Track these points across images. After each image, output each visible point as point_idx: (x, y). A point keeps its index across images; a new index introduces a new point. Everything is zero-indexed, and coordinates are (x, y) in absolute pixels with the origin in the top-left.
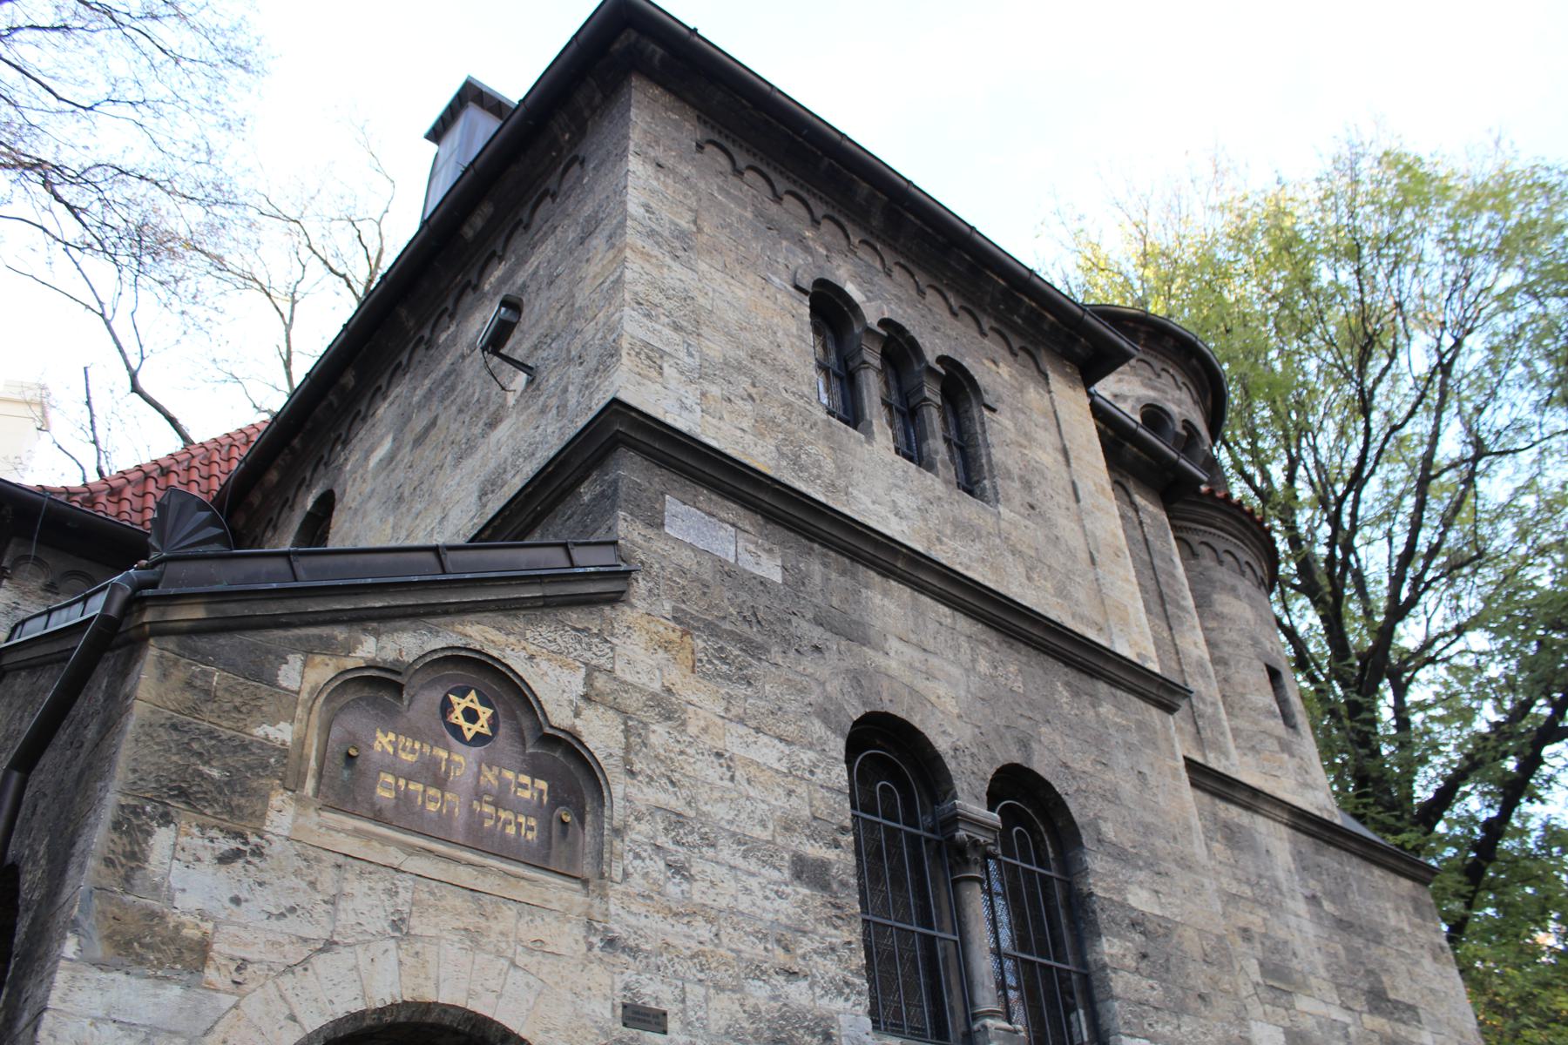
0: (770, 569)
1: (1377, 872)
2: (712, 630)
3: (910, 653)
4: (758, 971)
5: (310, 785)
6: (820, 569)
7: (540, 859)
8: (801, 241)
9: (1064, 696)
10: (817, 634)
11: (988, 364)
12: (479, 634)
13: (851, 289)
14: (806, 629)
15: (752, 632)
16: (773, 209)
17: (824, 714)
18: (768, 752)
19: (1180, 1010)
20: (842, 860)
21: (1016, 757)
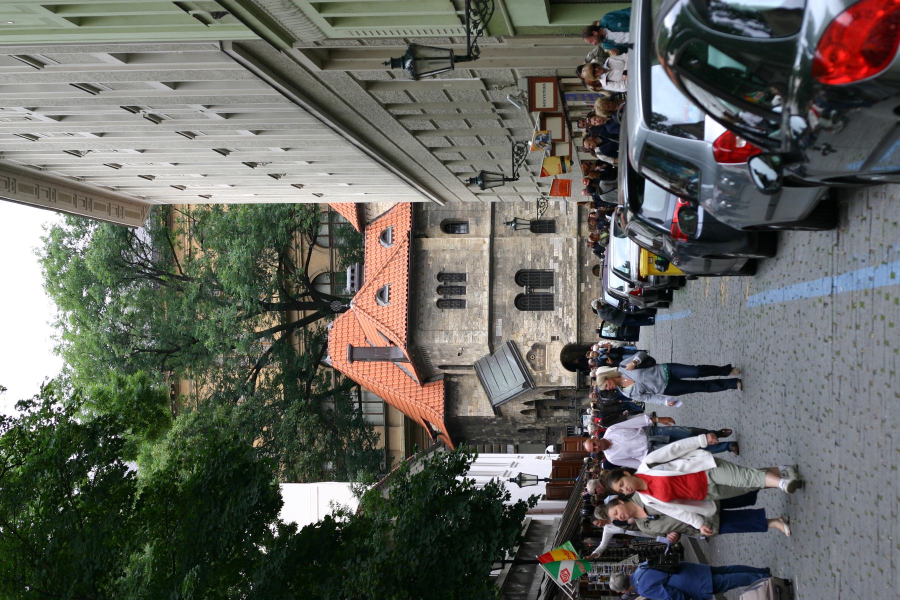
0: (500, 320)
2: (512, 330)
3: (504, 297)
4: (551, 325)
6: (497, 312)
7: (545, 349)
8: (430, 310)
9: (499, 266)
10: (507, 314)
12: (524, 357)
13: (435, 300)
14: (507, 315)
16: (426, 315)
17: (518, 314)
18: (526, 322)
19: (544, 254)
20: (536, 313)
21: (513, 280)
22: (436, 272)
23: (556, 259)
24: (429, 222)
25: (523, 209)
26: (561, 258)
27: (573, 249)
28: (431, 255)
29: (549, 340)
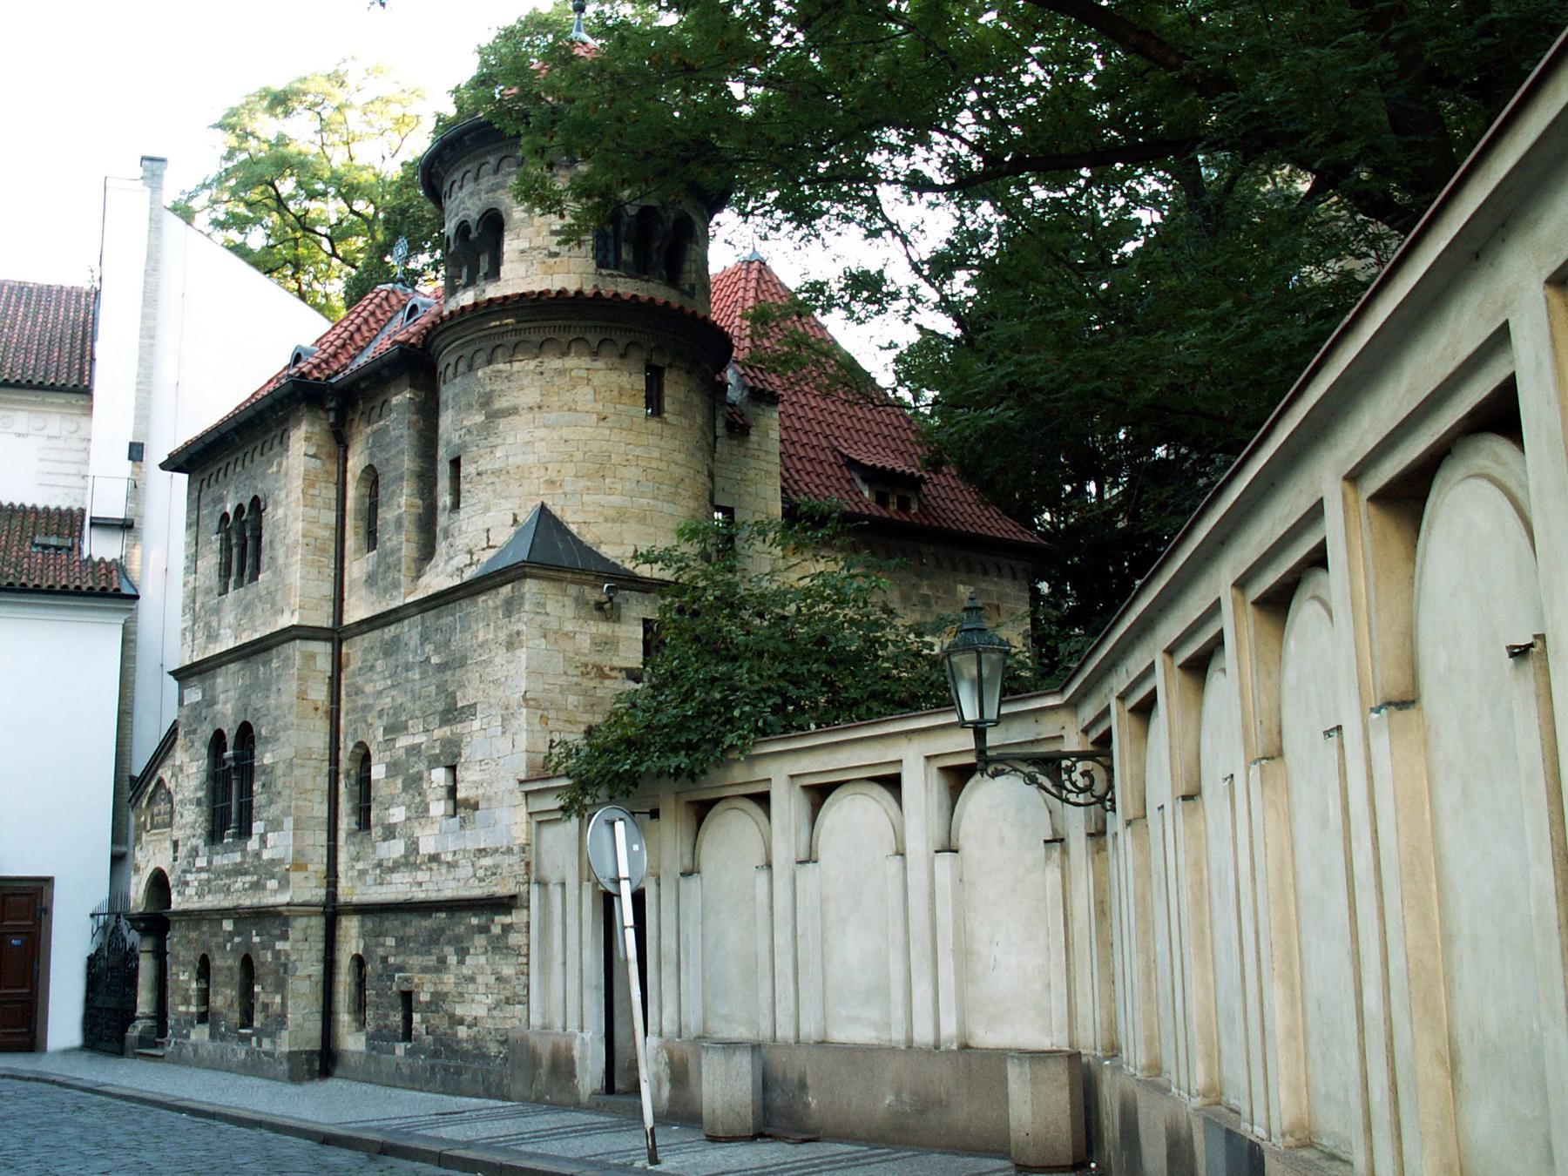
1: (482, 598)
4: (189, 838)
5: (148, 827)
11: (270, 471)
15: (194, 726)
22: (260, 488)
23: (263, 840)
24: (375, 427)
25: (385, 720)
26: (266, 855)
27: (275, 892)
28: (285, 463)
29: (177, 834)
